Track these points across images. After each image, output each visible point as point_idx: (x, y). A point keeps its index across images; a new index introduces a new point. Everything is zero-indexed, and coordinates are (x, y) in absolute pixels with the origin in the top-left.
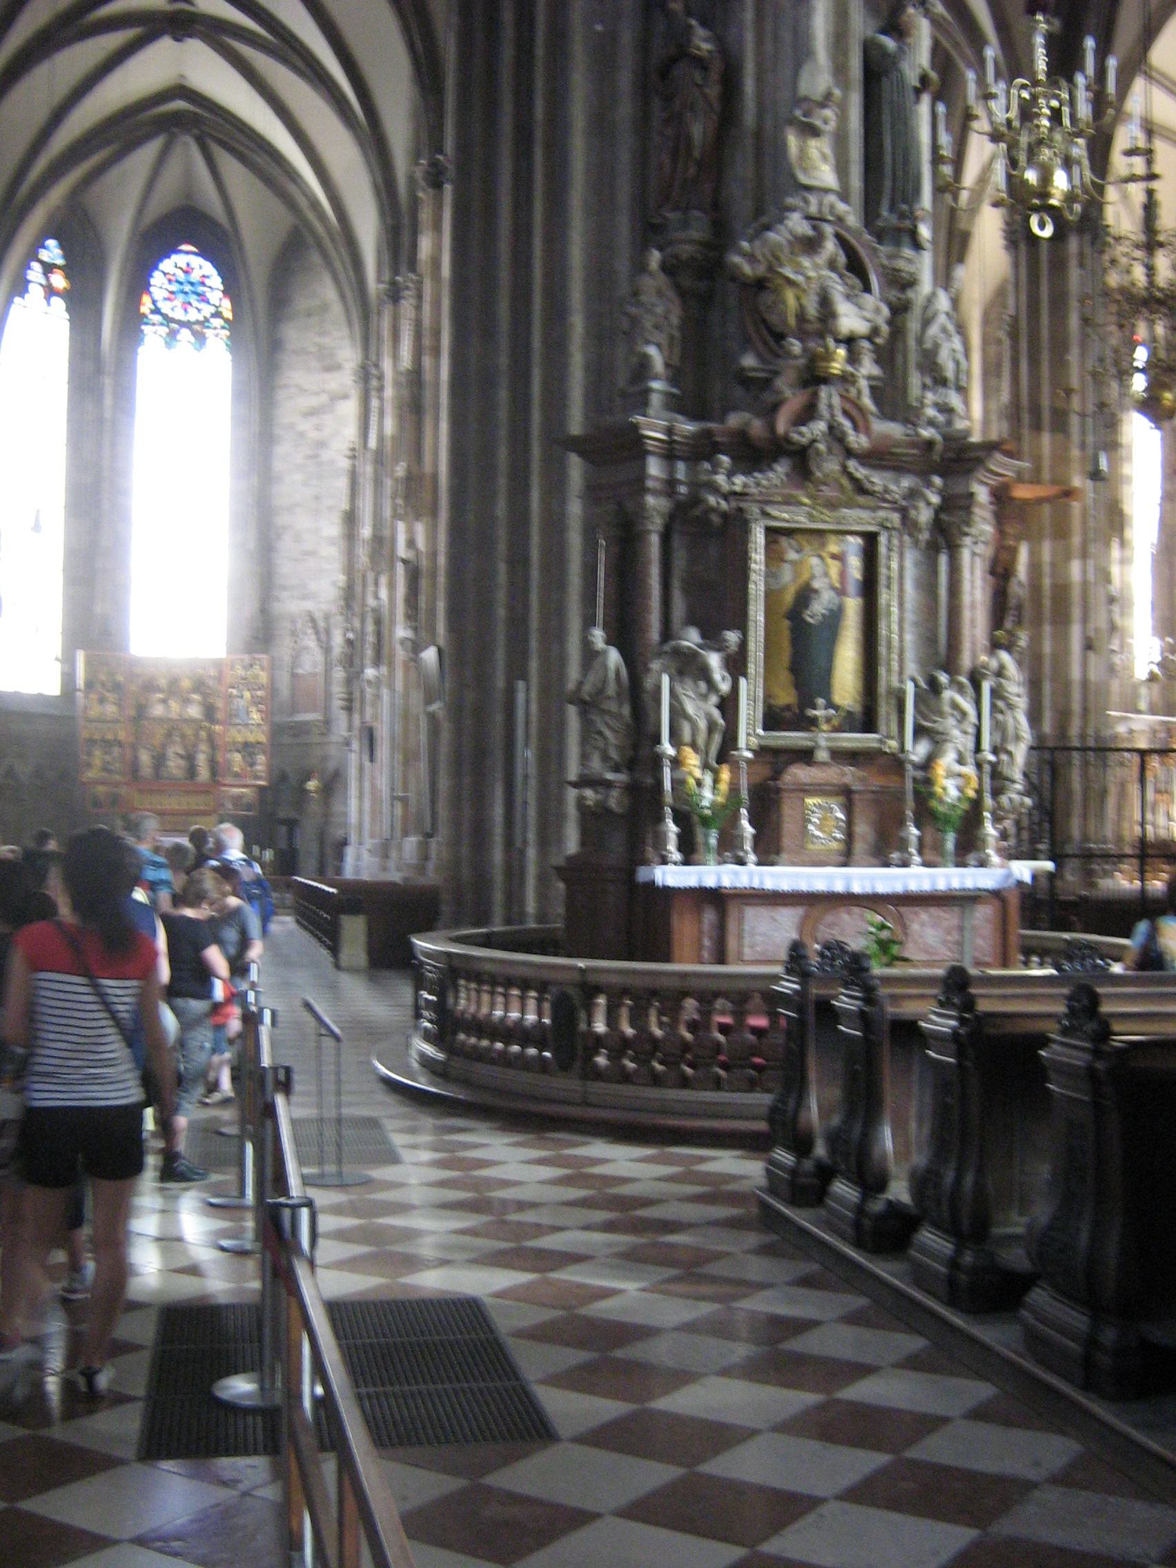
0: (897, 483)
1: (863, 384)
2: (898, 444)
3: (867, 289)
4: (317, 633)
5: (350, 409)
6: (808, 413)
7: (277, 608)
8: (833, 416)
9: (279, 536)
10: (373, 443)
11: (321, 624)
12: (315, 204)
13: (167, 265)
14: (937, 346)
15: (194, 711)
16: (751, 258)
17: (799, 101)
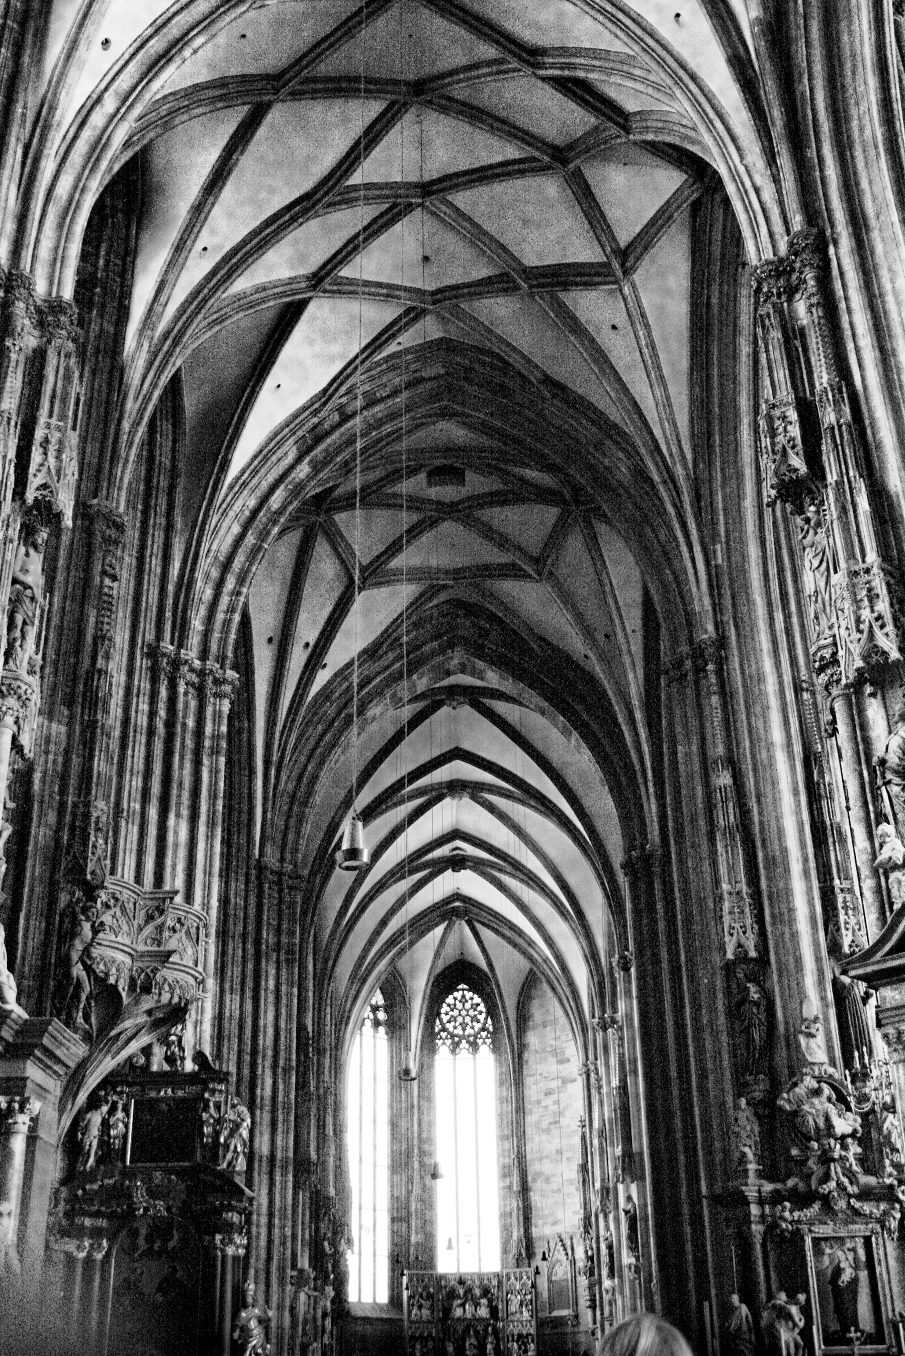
0: (878, 1208)
1: (852, 1159)
2: (875, 1188)
3: (849, 1109)
4: (565, 1249)
5: (577, 1089)
6: (826, 1178)
7: (535, 1232)
8: (838, 1178)
9: (534, 1180)
10: (596, 1124)
11: (568, 1243)
12: (546, 960)
13: (450, 1000)
14: (890, 1133)
15: (483, 1312)
16: (789, 1101)
17: (804, 1020)
